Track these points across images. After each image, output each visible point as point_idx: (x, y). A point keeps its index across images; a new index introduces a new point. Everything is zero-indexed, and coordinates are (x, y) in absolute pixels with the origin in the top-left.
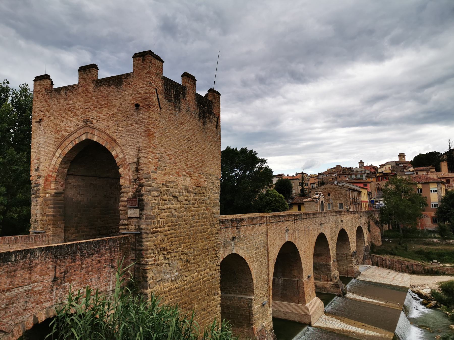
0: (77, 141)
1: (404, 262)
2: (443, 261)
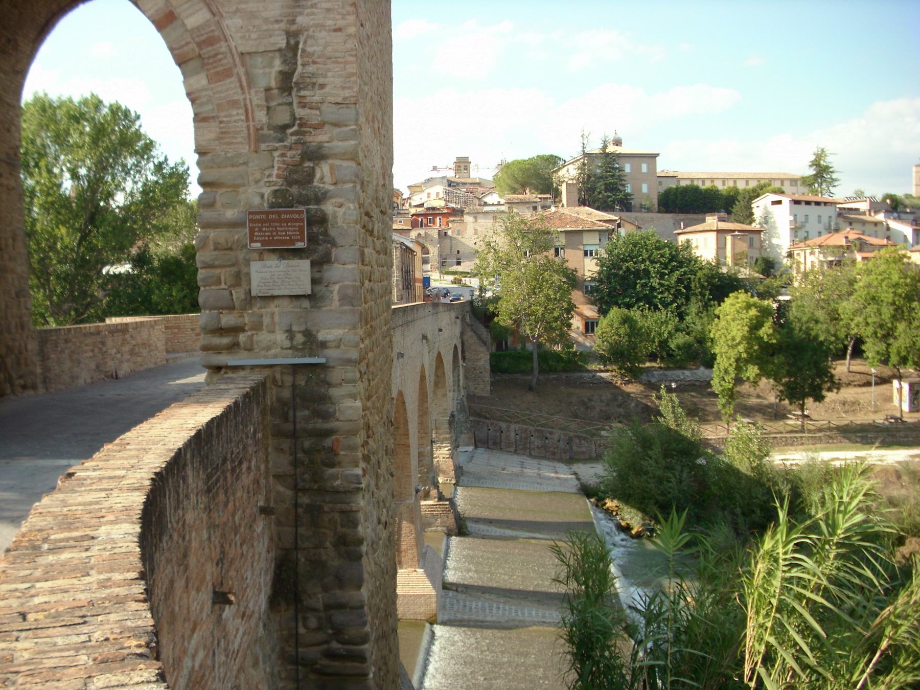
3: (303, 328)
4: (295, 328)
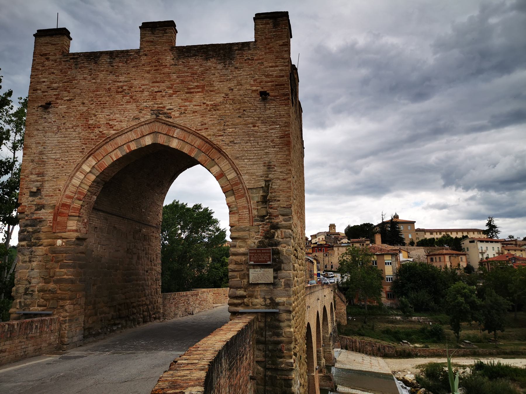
0: (133, 147)
1: (375, 344)
2: (413, 342)
3: (269, 297)
4: (266, 297)
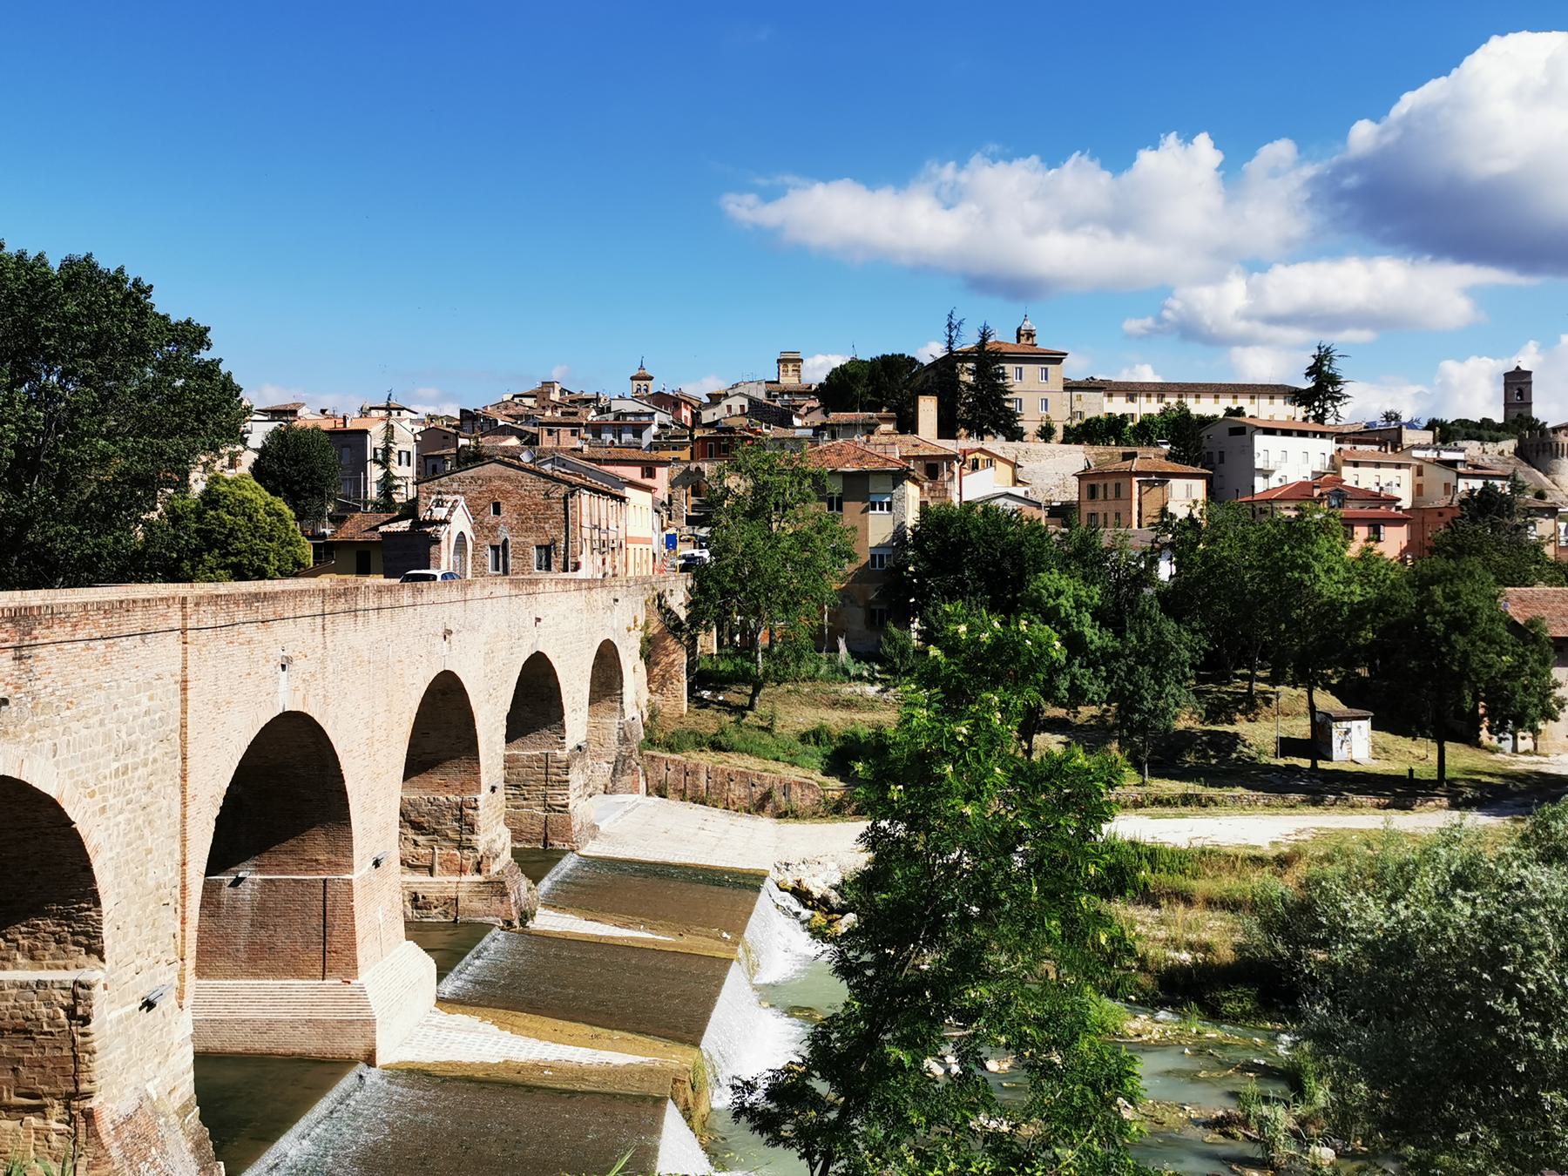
1: (759, 777)
